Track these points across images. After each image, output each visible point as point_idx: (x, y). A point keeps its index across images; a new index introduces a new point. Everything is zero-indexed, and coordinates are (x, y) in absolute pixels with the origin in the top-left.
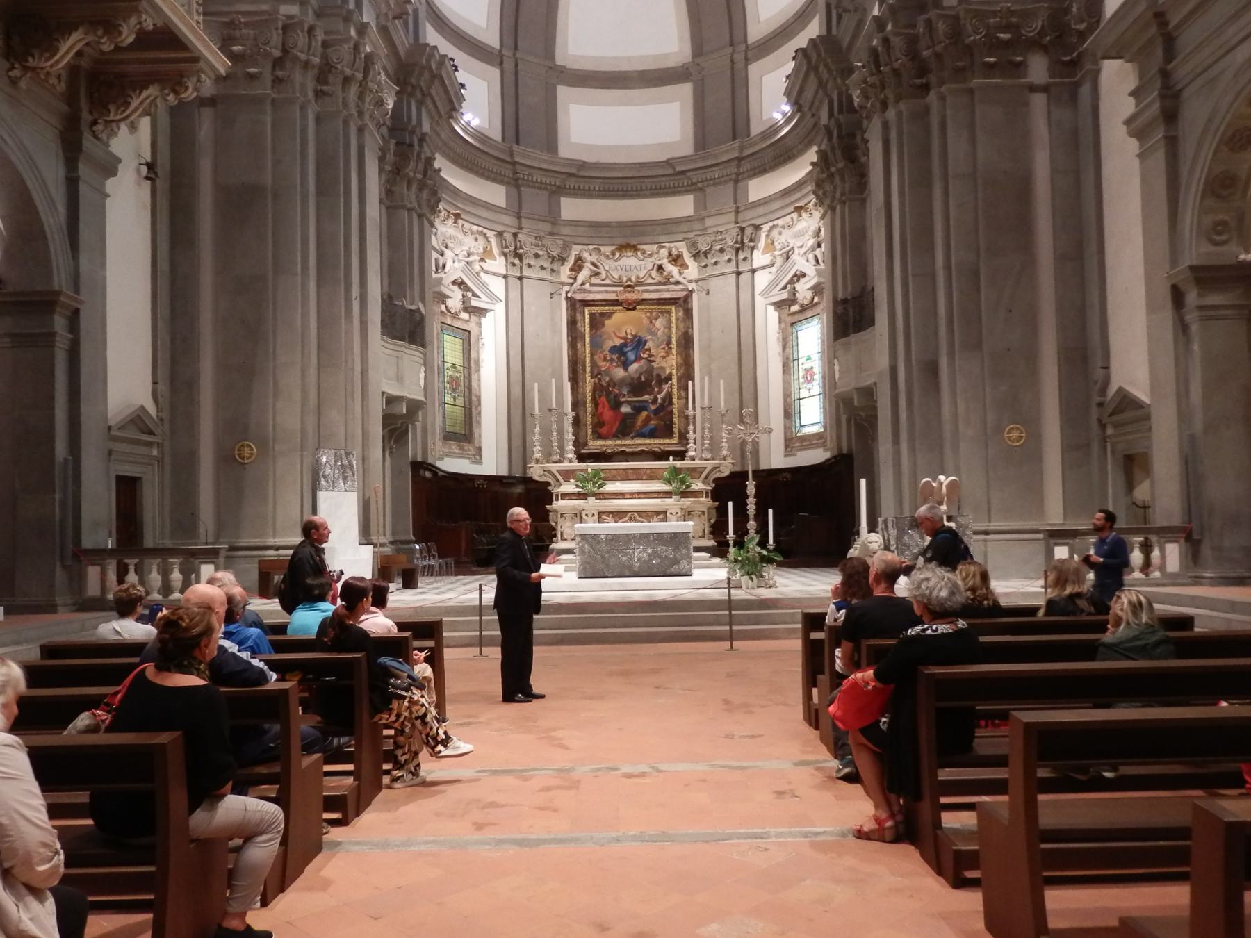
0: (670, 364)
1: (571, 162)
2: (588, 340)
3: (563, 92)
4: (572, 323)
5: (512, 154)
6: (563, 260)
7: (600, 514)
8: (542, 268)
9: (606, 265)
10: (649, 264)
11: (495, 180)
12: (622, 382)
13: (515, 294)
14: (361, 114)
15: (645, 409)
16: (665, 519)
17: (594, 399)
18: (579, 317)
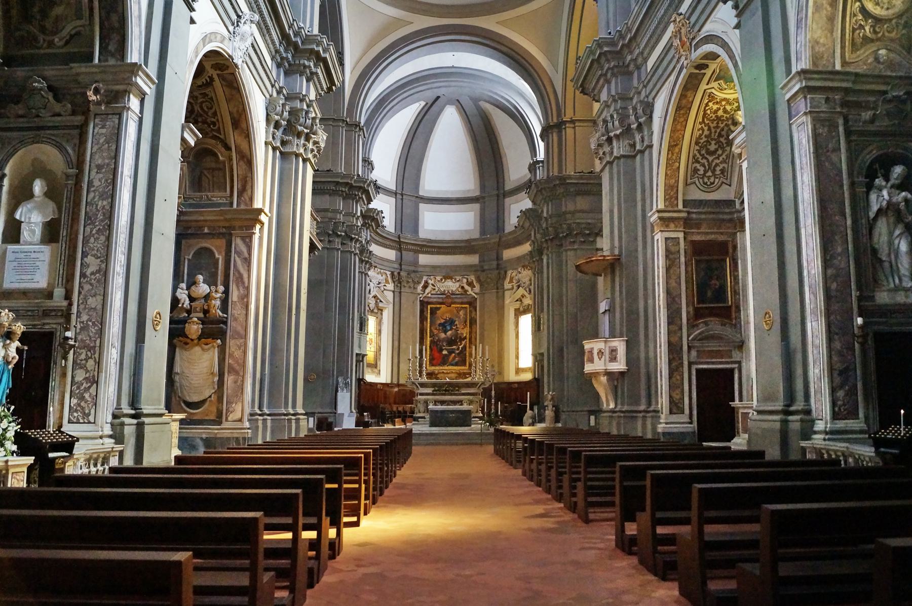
0: (465, 332)
1: (425, 240)
2: (429, 320)
3: (422, 206)
4: (422, 312)
5: (399, 238)
6: (419, 283)
7: (435, 402)
8: (410, 287)
9: (439, 285)
10: (457, 284)
11: (392, 249)
12: (444, 340)
13: (397, 299)
15: (454, 352)
16: (462, 405)
17: (430, 347)
18: (425, 309)
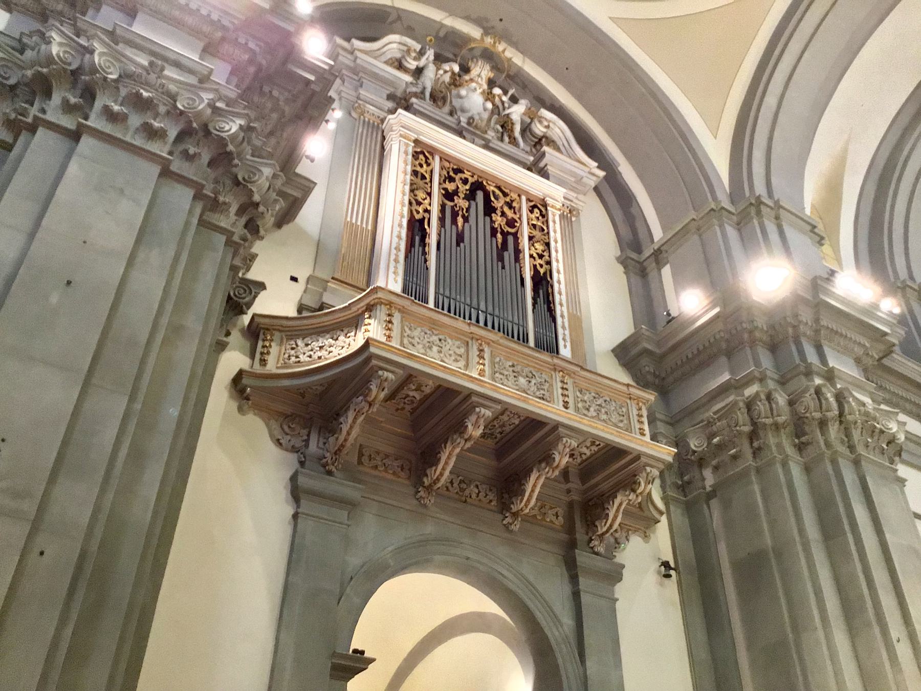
14: (852, 448)
